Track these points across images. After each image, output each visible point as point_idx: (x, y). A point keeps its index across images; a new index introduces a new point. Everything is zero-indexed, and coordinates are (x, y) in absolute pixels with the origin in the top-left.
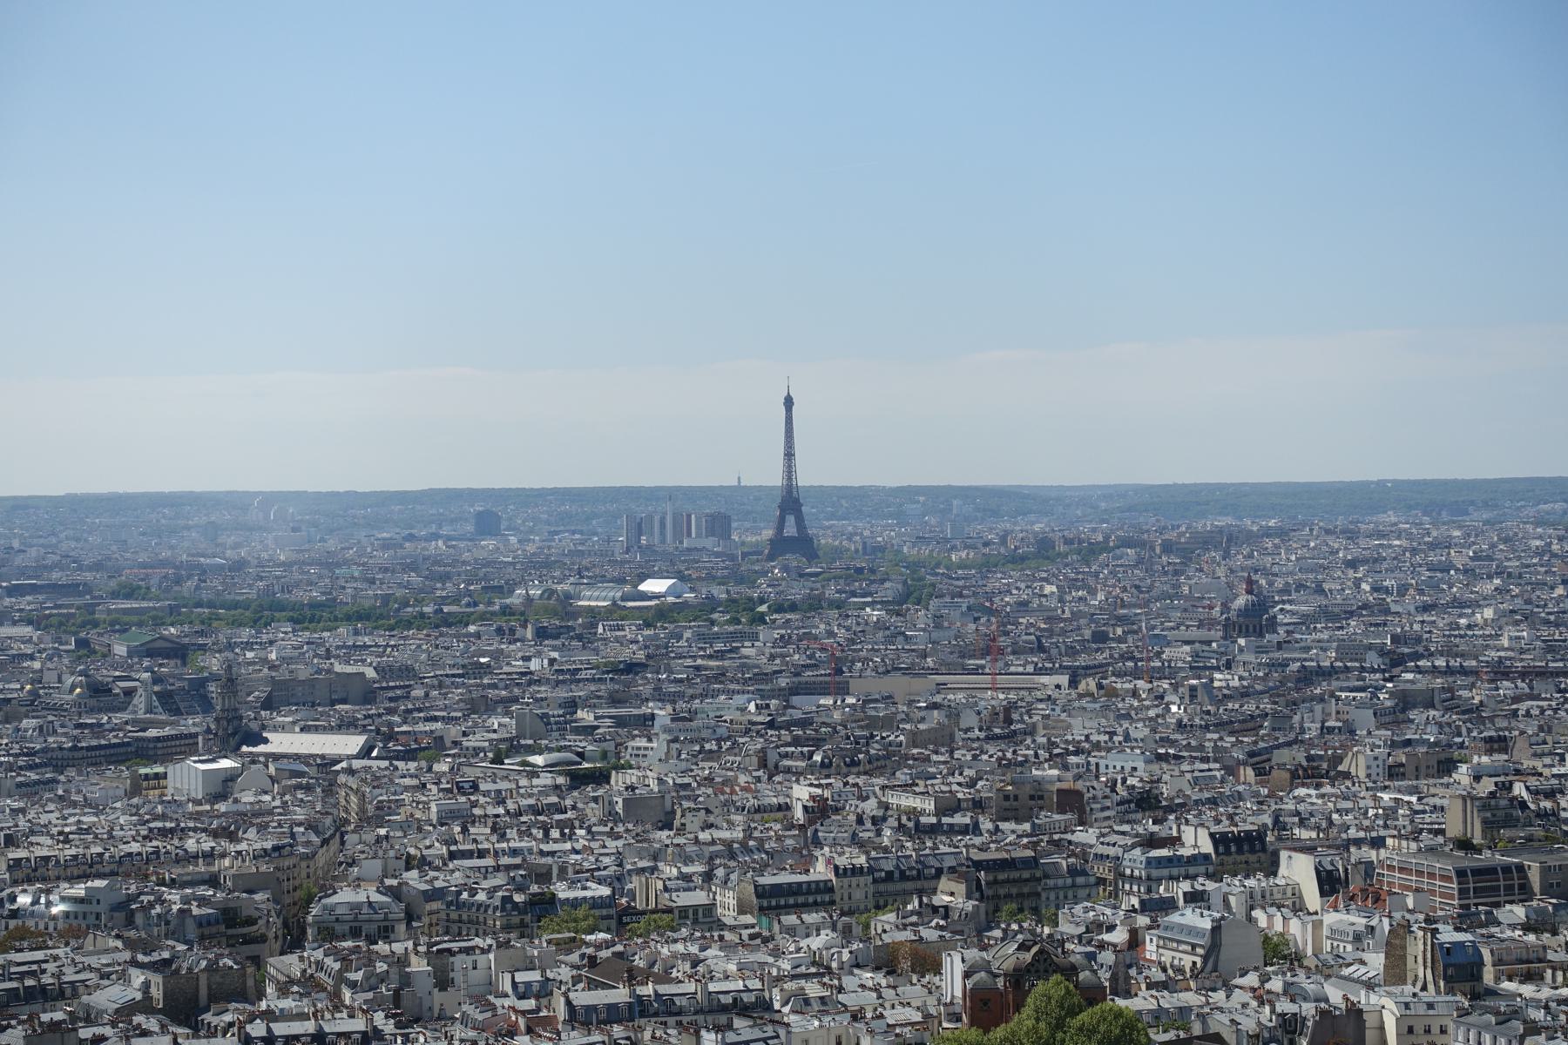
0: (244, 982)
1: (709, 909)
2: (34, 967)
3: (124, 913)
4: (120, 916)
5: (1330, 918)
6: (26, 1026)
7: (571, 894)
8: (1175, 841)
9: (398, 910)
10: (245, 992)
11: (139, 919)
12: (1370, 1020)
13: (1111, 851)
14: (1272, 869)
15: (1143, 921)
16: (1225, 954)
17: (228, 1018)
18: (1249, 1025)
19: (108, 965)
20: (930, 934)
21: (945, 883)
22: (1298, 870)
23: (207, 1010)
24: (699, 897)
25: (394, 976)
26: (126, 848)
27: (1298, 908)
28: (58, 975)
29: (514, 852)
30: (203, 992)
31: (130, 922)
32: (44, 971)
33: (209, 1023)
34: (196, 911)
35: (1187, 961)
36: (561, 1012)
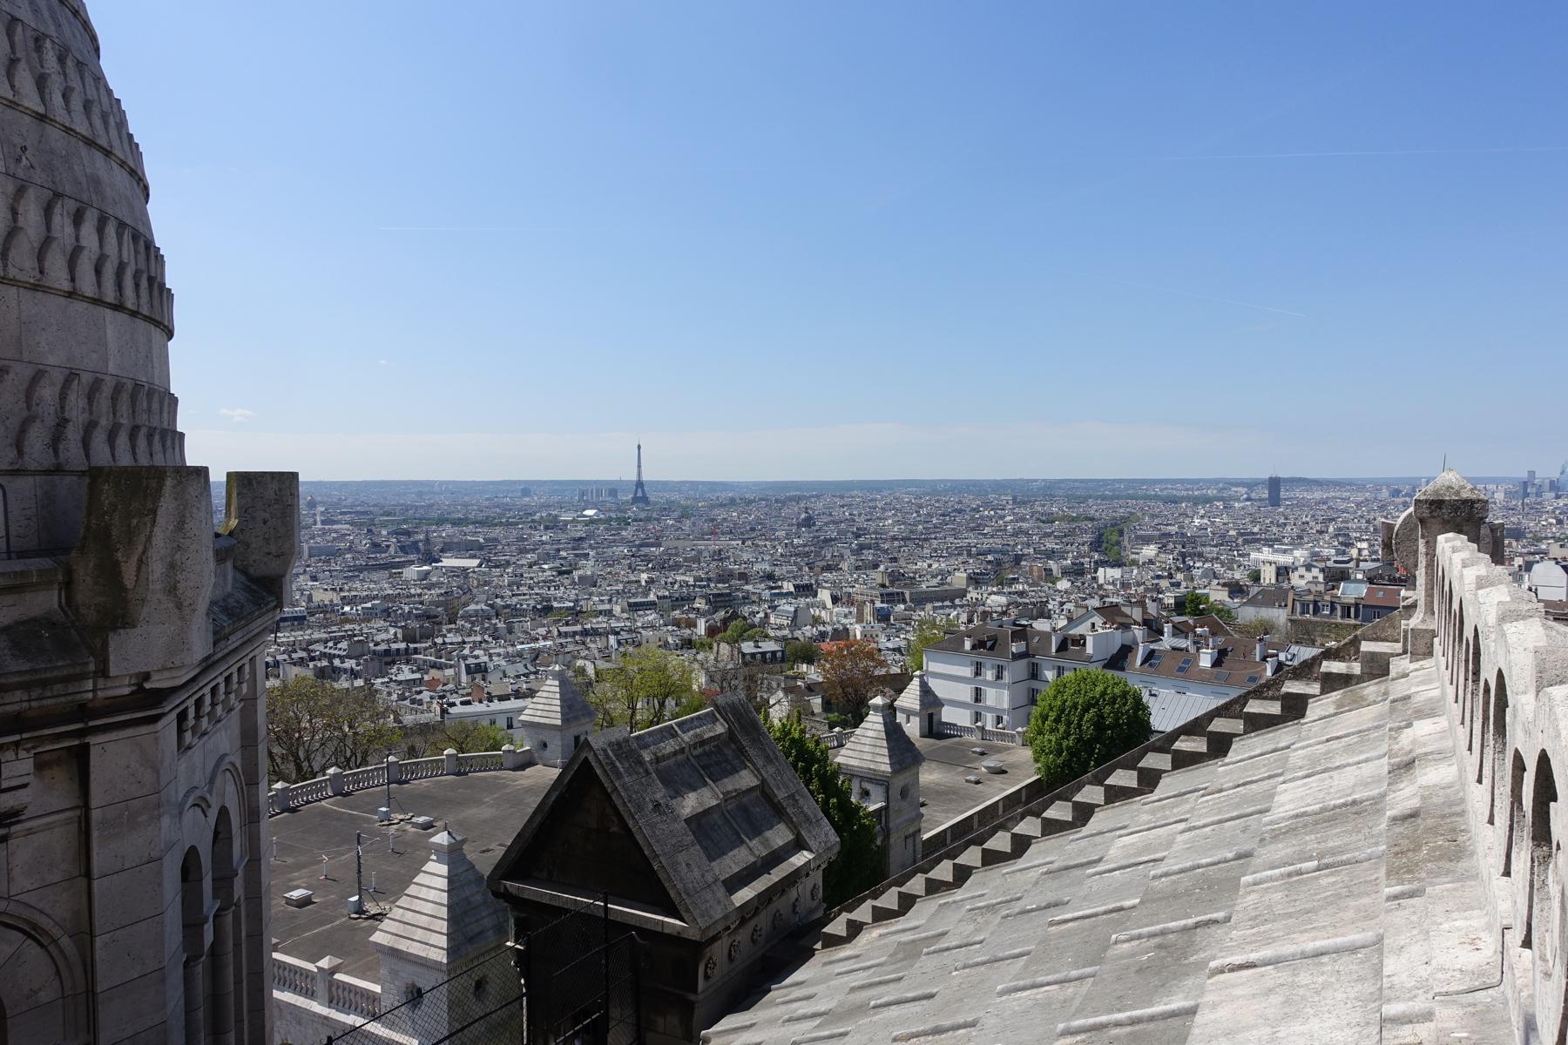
1: (610, 611)
3: (386, 613)
4: (385, 614)
5: (836, 610)
7: (559, 605)
8: (781, 587)
9: (493, 612)
11: (393, 615)
12: (851, 633)
13: (758, 591)
14: (815, 595)
15: (769, 611)
16: (799, 619)
18: (808, 634)
20: (692, 616)
21: (697, 600)
22: (824, 595)
24: (607, 607)
25: (492, 628)
26: (387, 592)
27: (825, 608)
29: (537, 594)
31: (389, 616)
34: (414, 612)
35: (785, 622)
36: (556, 633)
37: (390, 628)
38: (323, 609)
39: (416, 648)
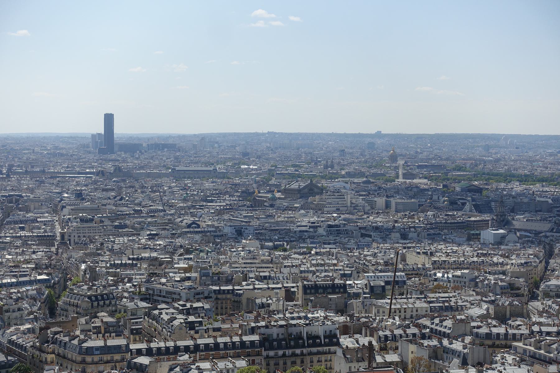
0: (523, 311)
2: (447, 299)
3: (474, 283)
4: (473, 283)
6: (453, 320)
10: (524, 314)
11: (480, 285)
17: (518, 323)
19: (473, 300)
23: (510, 319)
26: (472, 259)
28: (456, 303)
30: (508, 313)
31: (476, 285)
32: (451, 301)
33: (510, 324)
34: (500, 283)
37: (483, 304)
38: (415, 272)
39: (514, 335)
